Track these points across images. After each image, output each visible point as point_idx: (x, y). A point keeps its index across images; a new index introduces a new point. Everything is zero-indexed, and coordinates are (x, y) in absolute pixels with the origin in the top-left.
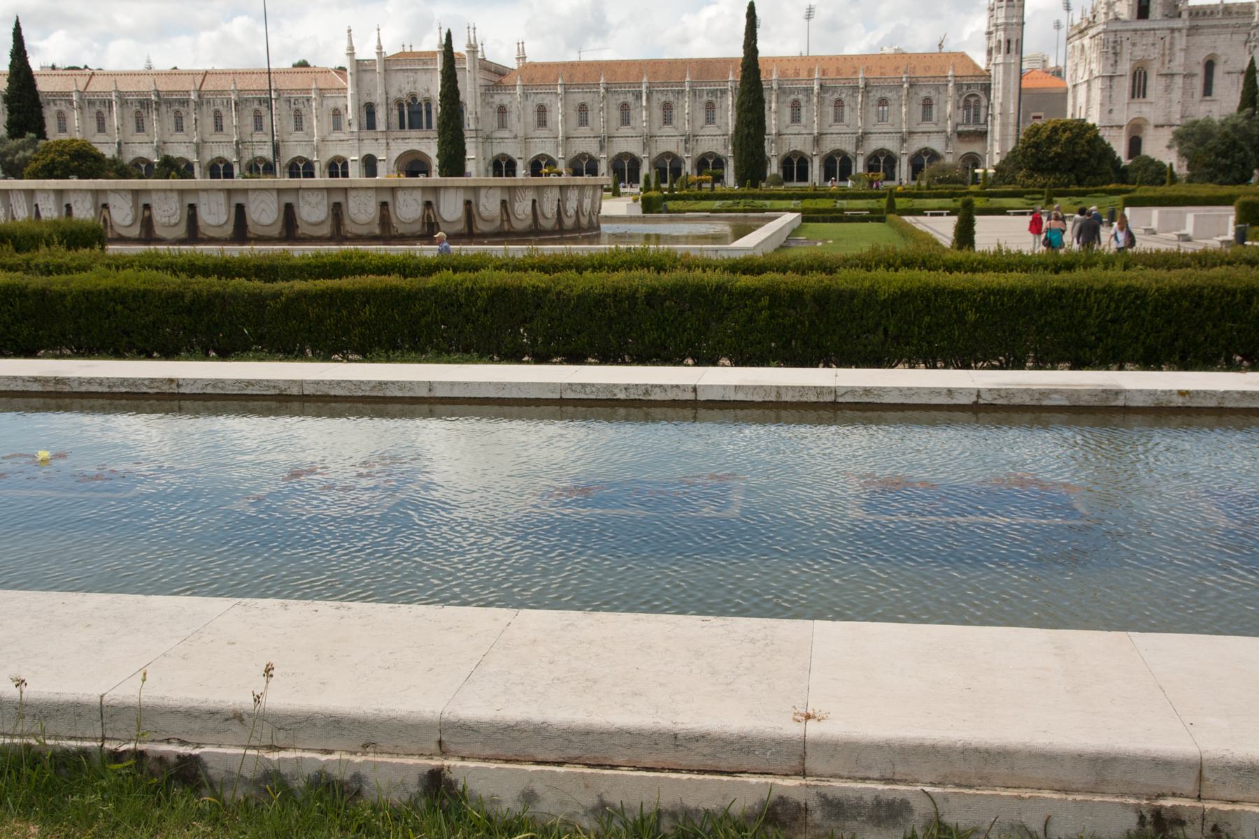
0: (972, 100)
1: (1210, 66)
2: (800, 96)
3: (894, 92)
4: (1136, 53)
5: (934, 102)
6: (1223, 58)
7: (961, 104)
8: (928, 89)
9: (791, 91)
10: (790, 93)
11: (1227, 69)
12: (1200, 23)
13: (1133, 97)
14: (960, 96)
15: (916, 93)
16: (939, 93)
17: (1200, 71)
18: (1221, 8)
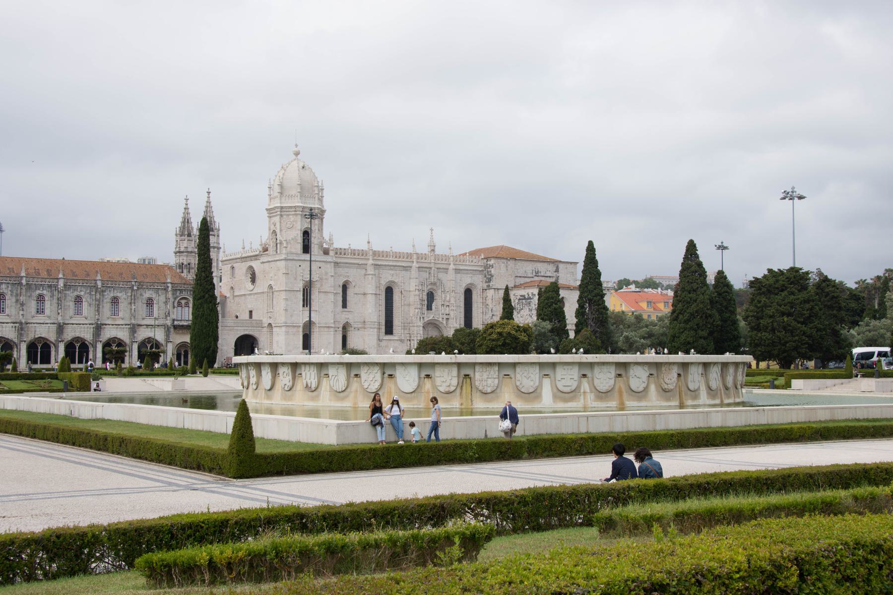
0: (183, 302)
1: (345, 288)
2: (45, 292)
3: (124, 293)
4: (305, 276)
5: (155, 302)
6: (354, 284)
7: (176, 305)
8: (151, 292)
9: (37, 287)
10: (36, 289)
11: (357, 290)
12: (339, 260)
13: (304, 306)
14: (175, 299)
15: (141, 295)
16: (159, 295)
17: (340, 290)
18: (350, 251)
